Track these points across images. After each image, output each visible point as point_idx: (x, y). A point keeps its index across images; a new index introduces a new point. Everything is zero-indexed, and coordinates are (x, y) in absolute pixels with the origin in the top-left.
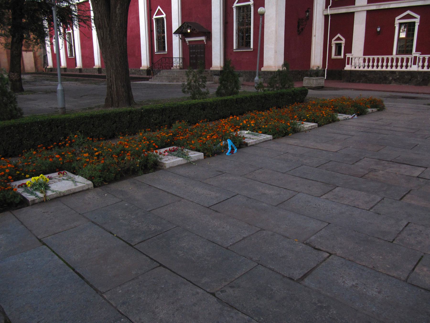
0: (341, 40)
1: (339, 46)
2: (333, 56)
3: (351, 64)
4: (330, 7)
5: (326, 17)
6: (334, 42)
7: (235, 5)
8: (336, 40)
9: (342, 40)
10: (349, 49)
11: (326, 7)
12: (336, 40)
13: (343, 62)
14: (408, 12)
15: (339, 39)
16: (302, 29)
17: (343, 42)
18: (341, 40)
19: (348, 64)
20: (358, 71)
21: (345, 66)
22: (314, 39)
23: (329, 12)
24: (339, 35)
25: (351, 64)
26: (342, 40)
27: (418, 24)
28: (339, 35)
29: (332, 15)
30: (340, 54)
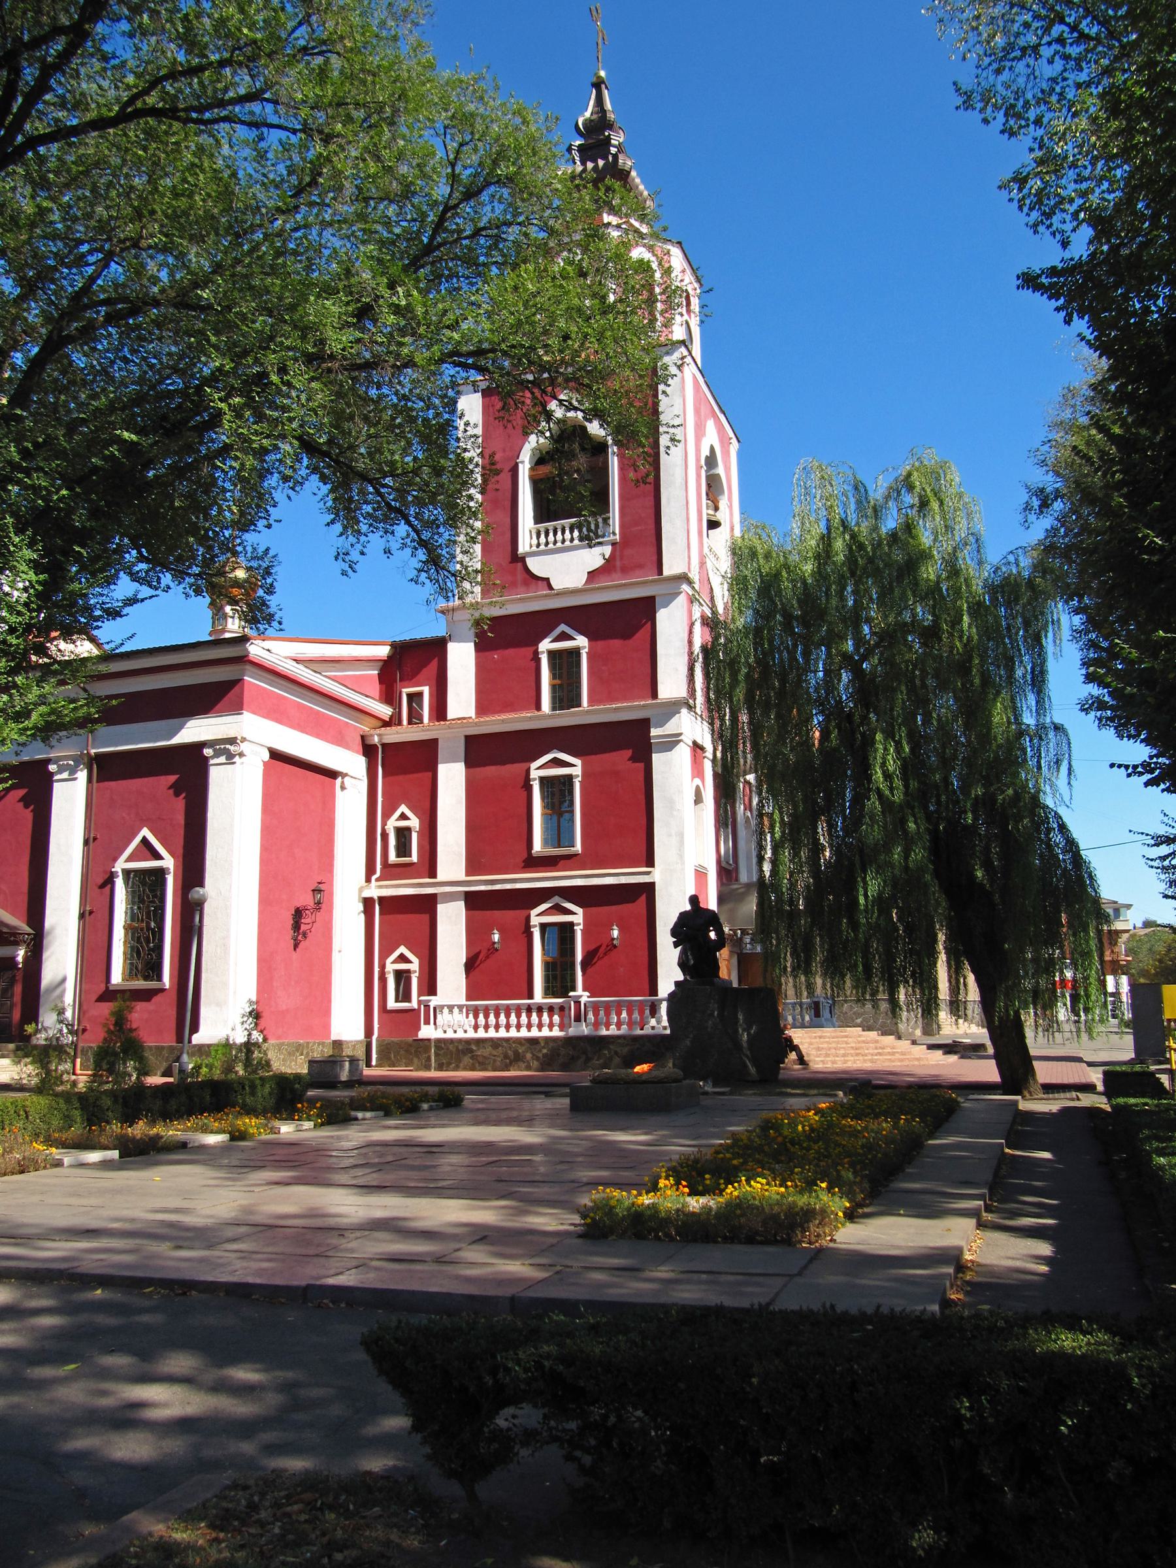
0: (408, 961)
1: (402, 977)
2: (392, 1004)
3: (435, 1023)
4: (377, 880)
5: (368, 903)
6: (390, 967)
7: (120, 865)
8: (394, 962)
9: (410, 962)
10: (430, 987)
11: (368, 880)
12: (394, 962)
13: (411, 1019)
14: (556, 899)
15: (403, 959)
16: (305, 935)
17: (415, 965)
18: (408, 961)
19: (427, 1022)
20: (452, 1041)
21: (419, 1029)
22: (336, 957)
23: (375, 891)
24: (402, 950)
25: (435, 1023)
26: (410, 962)
27: (581, 927)
28: (402, 950)
29: (381, 899)
30: (407, 997)
